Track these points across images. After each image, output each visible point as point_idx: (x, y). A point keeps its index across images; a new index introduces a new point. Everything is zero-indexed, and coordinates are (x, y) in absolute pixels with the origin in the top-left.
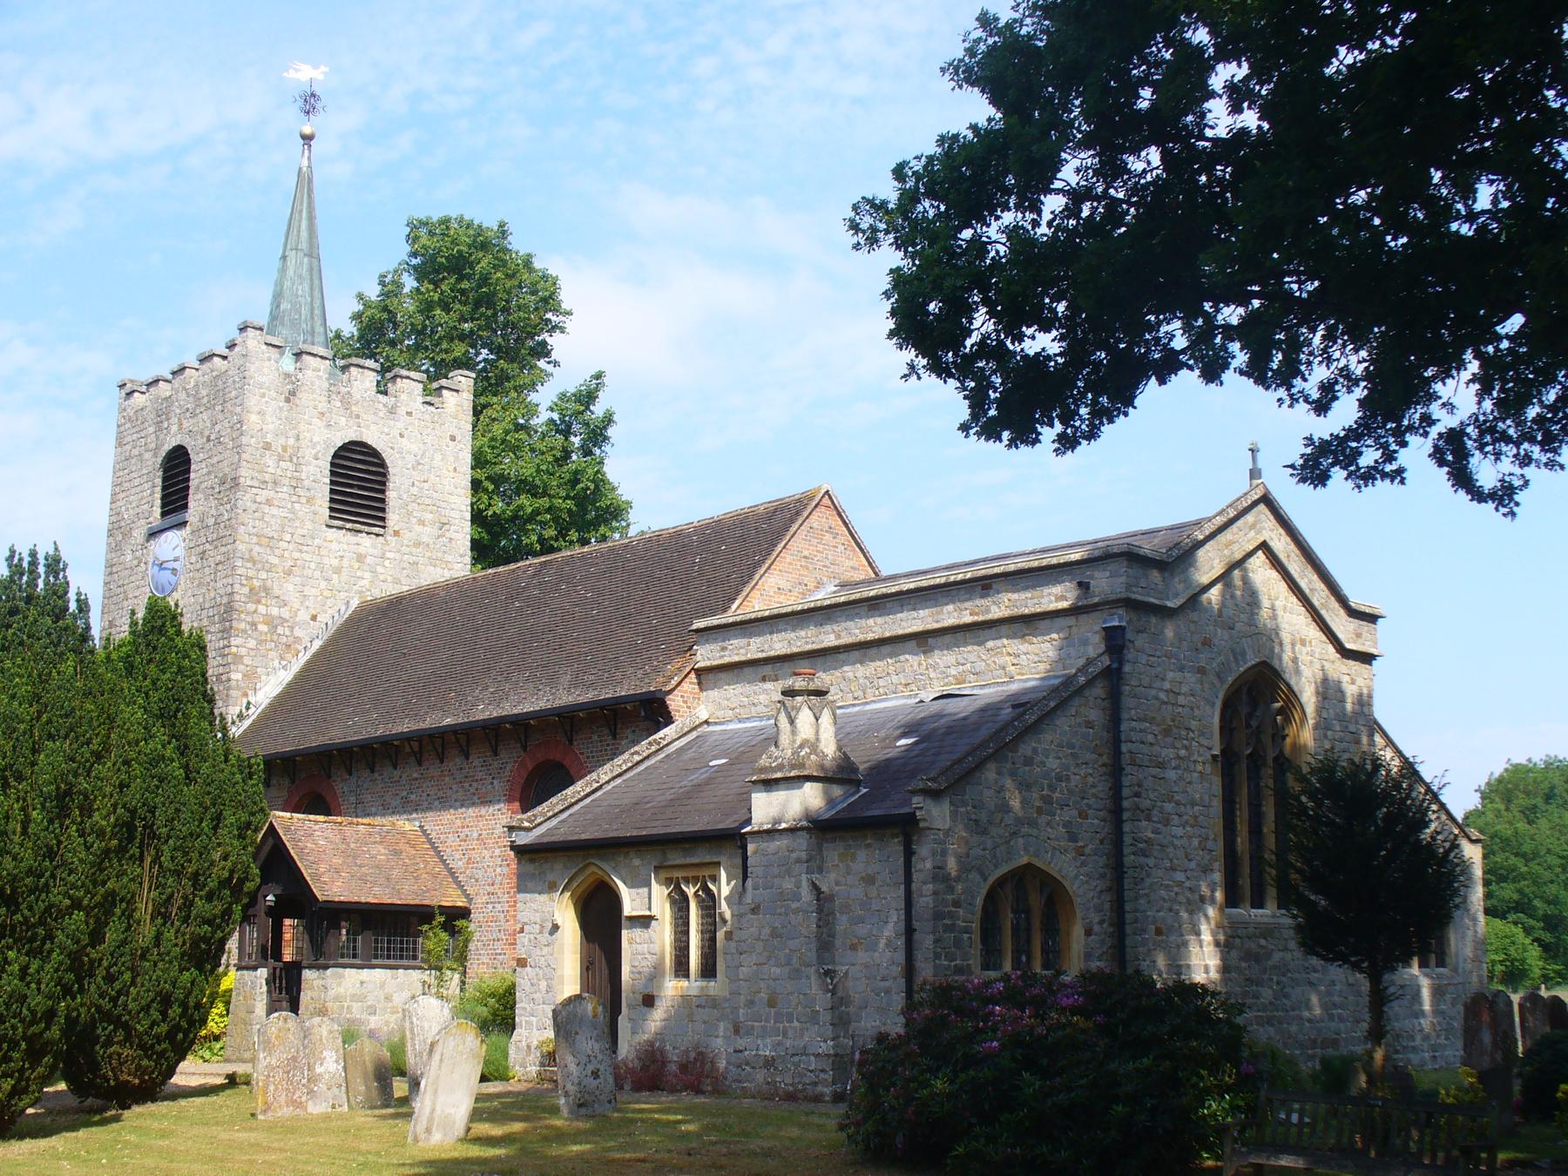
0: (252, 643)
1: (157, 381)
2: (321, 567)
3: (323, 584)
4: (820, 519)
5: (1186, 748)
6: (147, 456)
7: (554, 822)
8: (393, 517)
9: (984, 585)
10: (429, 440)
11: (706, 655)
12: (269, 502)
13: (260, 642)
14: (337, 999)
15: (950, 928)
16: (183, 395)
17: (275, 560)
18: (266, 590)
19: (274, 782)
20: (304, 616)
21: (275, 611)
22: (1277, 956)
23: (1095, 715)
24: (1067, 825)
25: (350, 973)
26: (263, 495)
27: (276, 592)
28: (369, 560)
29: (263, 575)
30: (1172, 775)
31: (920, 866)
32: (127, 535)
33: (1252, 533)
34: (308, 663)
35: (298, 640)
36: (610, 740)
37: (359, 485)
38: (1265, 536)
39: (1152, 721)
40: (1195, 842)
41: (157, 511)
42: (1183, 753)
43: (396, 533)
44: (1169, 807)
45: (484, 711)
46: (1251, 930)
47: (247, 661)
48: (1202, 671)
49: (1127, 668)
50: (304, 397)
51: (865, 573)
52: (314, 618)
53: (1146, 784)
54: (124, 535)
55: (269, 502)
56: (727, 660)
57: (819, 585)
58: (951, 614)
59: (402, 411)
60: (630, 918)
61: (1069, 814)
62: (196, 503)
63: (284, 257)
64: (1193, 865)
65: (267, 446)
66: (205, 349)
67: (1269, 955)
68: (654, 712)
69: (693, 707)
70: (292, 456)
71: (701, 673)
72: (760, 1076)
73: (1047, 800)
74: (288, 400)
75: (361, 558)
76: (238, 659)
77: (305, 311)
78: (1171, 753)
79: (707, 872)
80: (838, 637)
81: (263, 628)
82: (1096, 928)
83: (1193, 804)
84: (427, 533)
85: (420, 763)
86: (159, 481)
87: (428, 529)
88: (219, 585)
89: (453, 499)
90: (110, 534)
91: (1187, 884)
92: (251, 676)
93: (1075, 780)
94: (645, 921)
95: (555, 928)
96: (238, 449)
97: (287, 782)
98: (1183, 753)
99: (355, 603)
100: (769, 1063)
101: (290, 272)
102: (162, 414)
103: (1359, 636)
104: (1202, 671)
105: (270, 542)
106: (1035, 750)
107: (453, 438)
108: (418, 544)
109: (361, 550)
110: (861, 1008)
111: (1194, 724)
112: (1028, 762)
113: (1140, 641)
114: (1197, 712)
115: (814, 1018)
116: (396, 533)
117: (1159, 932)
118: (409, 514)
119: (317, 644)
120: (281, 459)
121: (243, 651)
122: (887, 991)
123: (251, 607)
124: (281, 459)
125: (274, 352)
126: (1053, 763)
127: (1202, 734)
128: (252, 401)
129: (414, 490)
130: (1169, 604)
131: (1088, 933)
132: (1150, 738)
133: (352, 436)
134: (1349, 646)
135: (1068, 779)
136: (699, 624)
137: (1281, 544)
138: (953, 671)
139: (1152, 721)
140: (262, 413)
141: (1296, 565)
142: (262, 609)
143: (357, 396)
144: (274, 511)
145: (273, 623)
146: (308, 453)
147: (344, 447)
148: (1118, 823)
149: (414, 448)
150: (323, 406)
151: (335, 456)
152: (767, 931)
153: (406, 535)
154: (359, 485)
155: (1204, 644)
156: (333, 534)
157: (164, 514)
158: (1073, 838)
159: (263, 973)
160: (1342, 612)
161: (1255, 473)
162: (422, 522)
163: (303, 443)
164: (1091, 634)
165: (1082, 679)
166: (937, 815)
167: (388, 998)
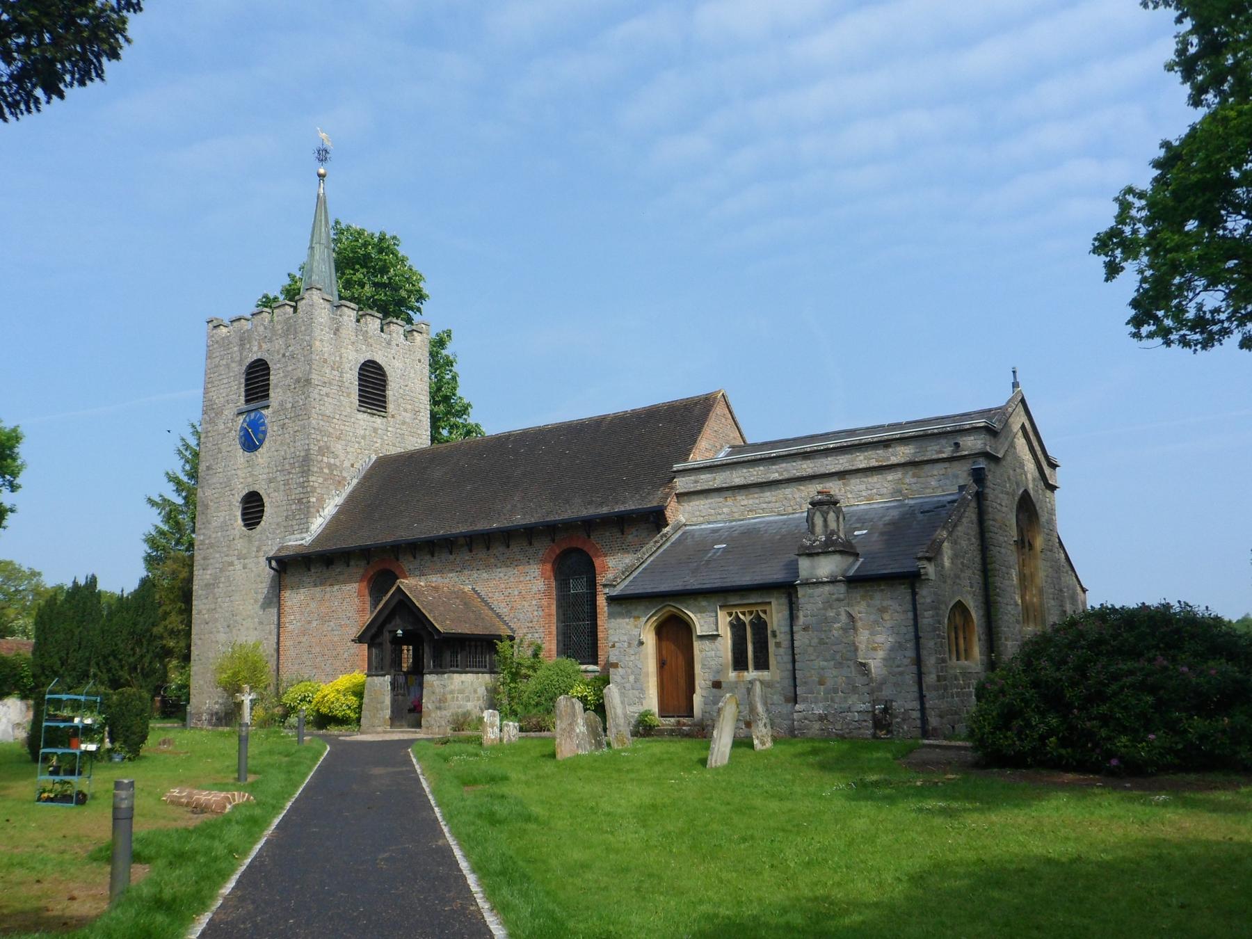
0: (321, 480)
1: (239, 319)
4: (719, 409)
6: (233, 365)
7: (627, 582)
8: (391, 407)
9: (886, 444)
10: (407, 361)
11: (681, 484)
12: (327, 395)
13: (325, 480)
14: (452, 692)
15: (939, 636)
16: (261, 329)
17: (331, 430)
18: (328, 448)
19: (352, 563)
20: (347, 464)
21: (332, 461)
23: (974, 517)
24: (970, 578)
25: (456, 676)
26: (325, 390)
31: (921, 601)
32: (219, 413)
34: (353, 492)
35: (344, 478)
36: (619, 535)
37: (373, 385)
41: (242, 399)
43: (393, 416)
45: (519, 519)
47: (318, 490)
49: (987, 491)
50: (343, 332)
51: (739, 442)
52: (352, 466)
54: (216, 414)
55: (327, 395)
56: (699, 488)
57: (722, 447)
58: (861, 460)
59: (394, 343)
60: (702, 637)
62: (275, 396)
63: (312, 248)
65: (325, 361)
68: (656, 519)
69: (680, 514)
70: (337, 367)
71: (679, 496)
72: (817, 726)
75: (375, 430)
76: (314, 489)
79: (759, 608)
80: (781, 474)
81: (326, 471)
84: (408, 416)
85: (471, 551)
86: (243, 380)
87: (408, 415)
88: (298, 444)
89: (421, 397)
90: (205, 413)
92: (321, 500)
94: (714, 637)
95: (641, 643)
96: (309, 363)
97: (363, 563)
99: (374, 458)
100: (821, 718)
101: (317, 257)
102: (244, 340)
104: (1007, 493)
105: (329, 419)
108: (404, 423)
110: (882, 684)
115: (855, 690)
119: (355, 481)
120: (333, 369)
121: (316, 484)
122: (901, 674)
123: (320, 458)
124: (333, 369)
125: (327, 305)
128: (317, 333)
133: (369, 357)
136: (677, 467)
138: (864, 494)
140: (322, 342)
142: (325, 459)
144: (330, 400)
145: (330, 466)
146: (347, 366)
149: (401, 366)
150: (353, 338)
151: (361, 369)
152: (815, 641)
154: (373, 385)
156: (361, 416)
157: (247, 401)
159: (388, 678)
162: (406, 410)
163: (344, 360)
164: (961, 473)
166: (930, 569)
167: (475, 691)
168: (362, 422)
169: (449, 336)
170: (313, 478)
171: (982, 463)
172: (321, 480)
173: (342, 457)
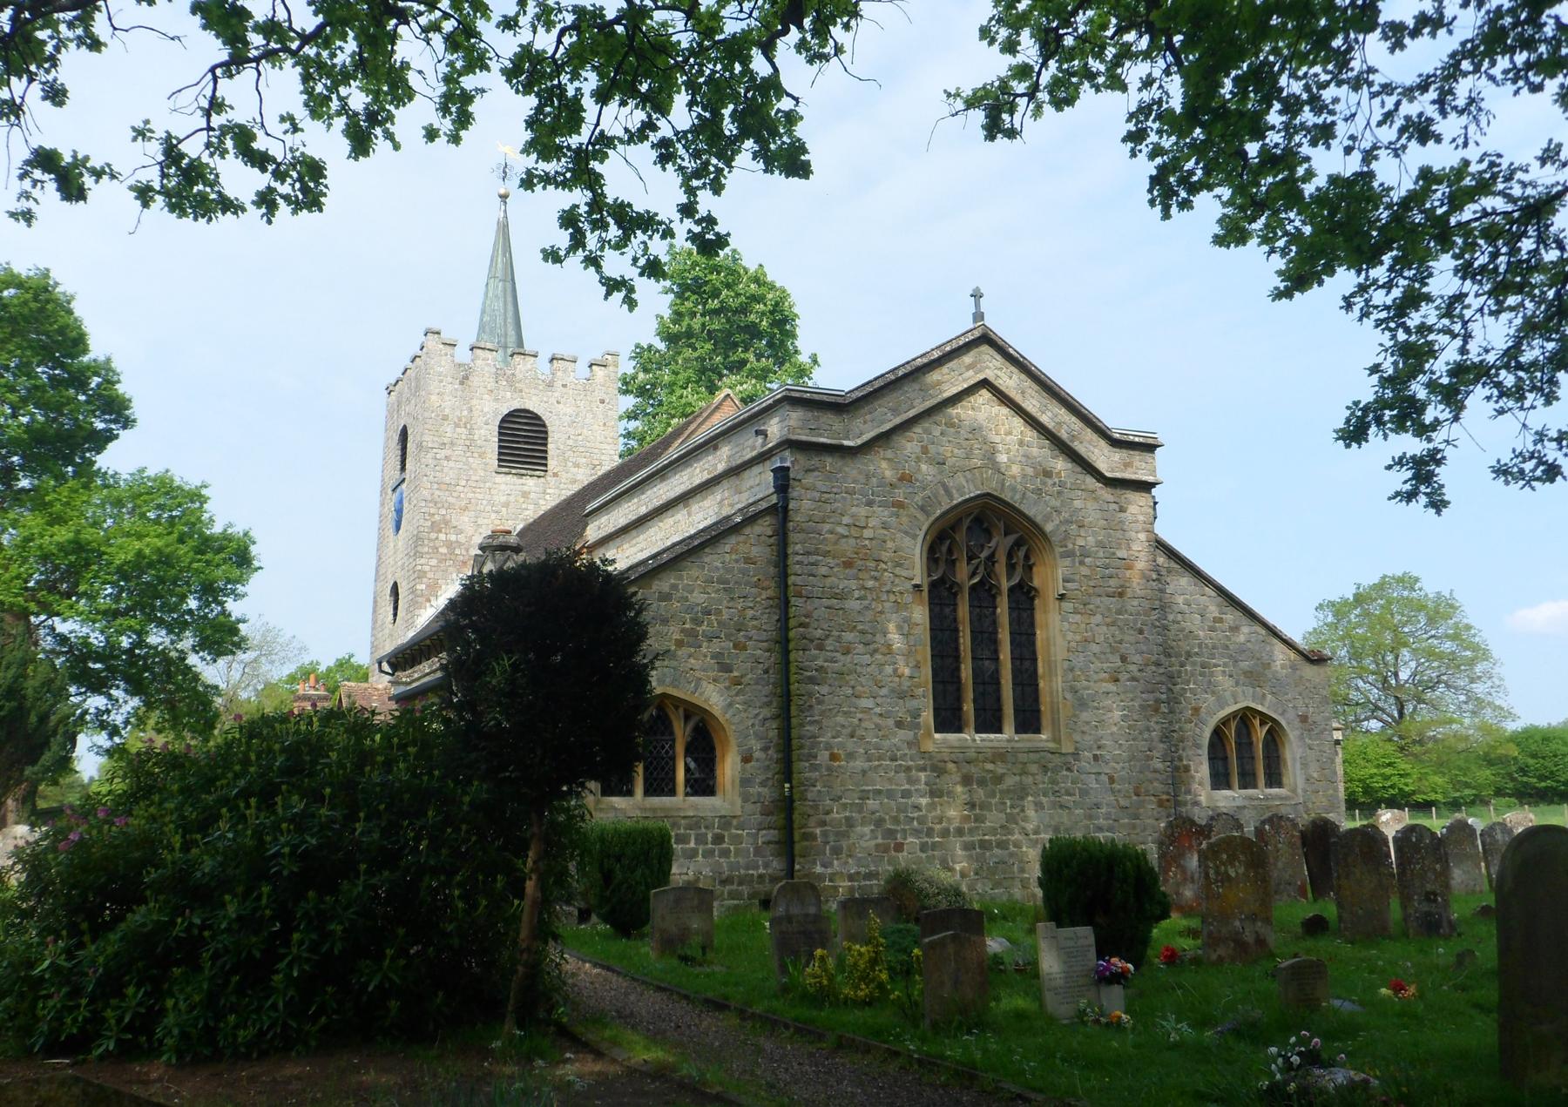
0: (434, 562)
2: (491, 503)
3: (493, 516)
5: (876, 579)
8: (552, 463)
12: (447, 458)
13: (440, 561)
17: (451, 500)
18: (447, 523)
21: (453, 538)
22: (1010, 781)
27: (454, 523)
28: (533, 496)
29: (443, 512)
30: (853, 604)
33: (971, 373)
38: (989, 374)
39: (826, 554)
42: (870, 584)
43: (555, 475)
44: (849, 636)
47: (430, 575)
50: (475, 380)
53: (815, 615)
55: (447, 458)
59: (558, 384)
61: (716, 646)
64: (884, 691)
65: (445, 418)
66: (411, 354)
67: (999, 779)
70: (468, 424)
73: (692, 633)
74: (462, 383)
75: (525, 495)
77: (499, 320)
78: (853, 584)
81: (443, 550)
82: (757, 754)
91: (878, 710)
98: (870, 584)
103: (1127, 465)
106: (674, 587)
107: (602, 402)
109: (526, 488)
111: (885, 555)
113: (809, 480)
114: (890, 544)
116: (555, 475)
117: (833, 757)
118: (566, 460)
121: (427, 568)
123: (433, 536)
124: (457, 426)
126: (698, 597)
127: (899, 565)
128: (434, 386)
129: (570, 442)
130: (846, 443)
131: (746, 759)
132: (823, 570)
133: (516, 405)
134: (1108, 475)
136: (589, 508)
137: (1010, 381)
139: (826, 554)
141: (1033, 402)
142: (442, 536)
143: (520, 376)
144: (451, 464)
145: (450, 545)
146: (480, 421)
147: (510, 414)
148: (786, 653)
149: (569, 410)
150: (491, 385)
151: (503, 421)
153: (564, 475)
156: (500, 479)
160: (1102, 443)
161: (979, 316)
162: (577, 465)
163: (476, 413)
165: (738, 520)
168: (503, 487)
169: (815, 362)
170: (423, 561)
171: (787, 459)
172: (434, 562)
173: (470, 530)
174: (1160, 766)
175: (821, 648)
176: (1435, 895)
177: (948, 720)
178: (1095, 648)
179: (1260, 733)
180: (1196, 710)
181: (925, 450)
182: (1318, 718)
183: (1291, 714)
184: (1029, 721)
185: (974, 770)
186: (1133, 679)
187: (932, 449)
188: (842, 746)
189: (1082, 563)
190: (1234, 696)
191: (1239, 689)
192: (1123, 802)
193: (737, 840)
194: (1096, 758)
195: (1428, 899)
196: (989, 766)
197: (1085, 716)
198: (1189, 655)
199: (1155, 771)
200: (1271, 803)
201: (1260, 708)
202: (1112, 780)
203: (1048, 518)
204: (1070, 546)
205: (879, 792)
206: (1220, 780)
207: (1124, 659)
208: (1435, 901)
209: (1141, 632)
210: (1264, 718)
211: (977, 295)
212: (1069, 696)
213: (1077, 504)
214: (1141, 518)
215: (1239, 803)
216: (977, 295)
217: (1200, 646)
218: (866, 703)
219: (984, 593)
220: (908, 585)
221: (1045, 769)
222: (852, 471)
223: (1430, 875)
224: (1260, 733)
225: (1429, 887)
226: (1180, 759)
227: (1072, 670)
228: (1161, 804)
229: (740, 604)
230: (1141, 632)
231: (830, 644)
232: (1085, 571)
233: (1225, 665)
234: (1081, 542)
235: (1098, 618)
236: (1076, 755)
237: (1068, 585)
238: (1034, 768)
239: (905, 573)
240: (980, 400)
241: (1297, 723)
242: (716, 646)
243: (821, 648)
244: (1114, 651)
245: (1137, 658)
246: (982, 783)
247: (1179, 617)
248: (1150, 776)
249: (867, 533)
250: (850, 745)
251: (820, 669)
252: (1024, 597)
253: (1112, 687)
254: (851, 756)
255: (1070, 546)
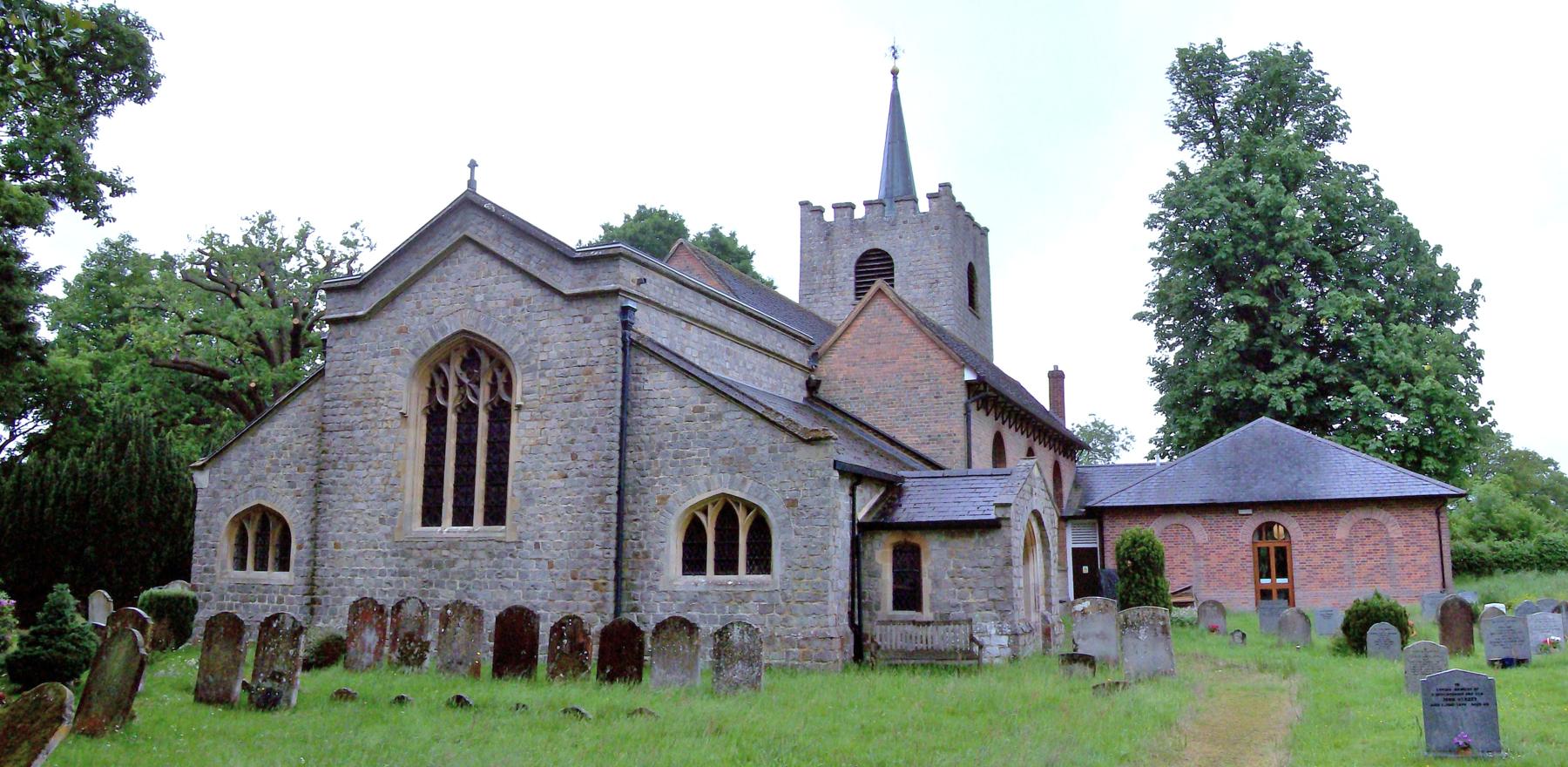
22: (461, 564)
30: (359, 433)
40: (378, 480)
44: (352, 457)
46: (431, 544)
48: (397, 353)
50: (836, 235)
61: (288, 471)
65: (814, 269)
67: (452, 563)
73: (275, 463)
78: (359, 419)
83: (378, 451)
93: (295, 447)
98: (370, 416)
111: (383, 393)
112: (264, 441)
113: (338, 346)
114: (388, 384)
117: (337, 546)
127: (391, 399)
131: (300, 547)
132: (341, 410)
133: (867, 247)
134: (567, 292)
135: (291, 447)
151: (859, 261)
155: (400, 331)
158: (292, 485)
160: (569, 265)
161: (472, 183)
162: (917, 287)
174: (599, 553)
175: (335, 467)
176: (281, 674)
177: (431, 515)
178: (546, 449)
179: (744, 522)
180: (664, 499)
181: (419, 305)
182: (809, 502)
183: (777, 498)
184: (496, 515)
185: (434, 555)
186: (582, 474)
187: (424, 303)
188: (342, 538)
189: (542, 376)
190: (708, 484)
191: (715, 477)
192: (559, 585)
193: (291, 602)
194: (537, 545)
195: (273, 677)
196: (445, 553)
197: (531, 509)
198: (660, 446)
199: (594, 557)
200: (739, 589)
201: (737, 494)
202: (551, 566)
203: (514, 341)
204: (533, 362)
205: (363, 571)
206: (693, 563)
207: (574, 457)
208: (280, 681)
209: (594, 430)
210: (749, 507)
211: (473, 165)
212: (517, 493)
213: (543, 324)
214: (605, 325)
215: (701, 588)
216: (473, 165)
217: (675, 438)
218: (360, 506)
219: (468, 413)
220: (397, 414)
221: (491, 555)
222: (366, 335)
223: (282, 658)
224: (744, 522)
225: (277, 668)
226: (641, 546)
227: (524, 470)
228: (596, 588)
229: (304, 440)
230: (594, 430)
231: (340, 464)
232: (544, 382)
233: (701, 453)
234: (543, 357)
235: (554, 421)
236: (519, 543)
237: (527, 397)
238: (481, 554)
239: (395, 405)
240: (466, 254)
241: (782, 508)
242: (288, 471)
243: (335, 467)
244: (565, 450)
245: (589, 456)
246: (438, 566)
247: (655, 411)
248: (588, 561)
249: (372, 378)
250: (348, 537)
251: (333, 483)
252: (501, 414)
253: (560, 483)
254: (349, 544)
255: (533, 362)
